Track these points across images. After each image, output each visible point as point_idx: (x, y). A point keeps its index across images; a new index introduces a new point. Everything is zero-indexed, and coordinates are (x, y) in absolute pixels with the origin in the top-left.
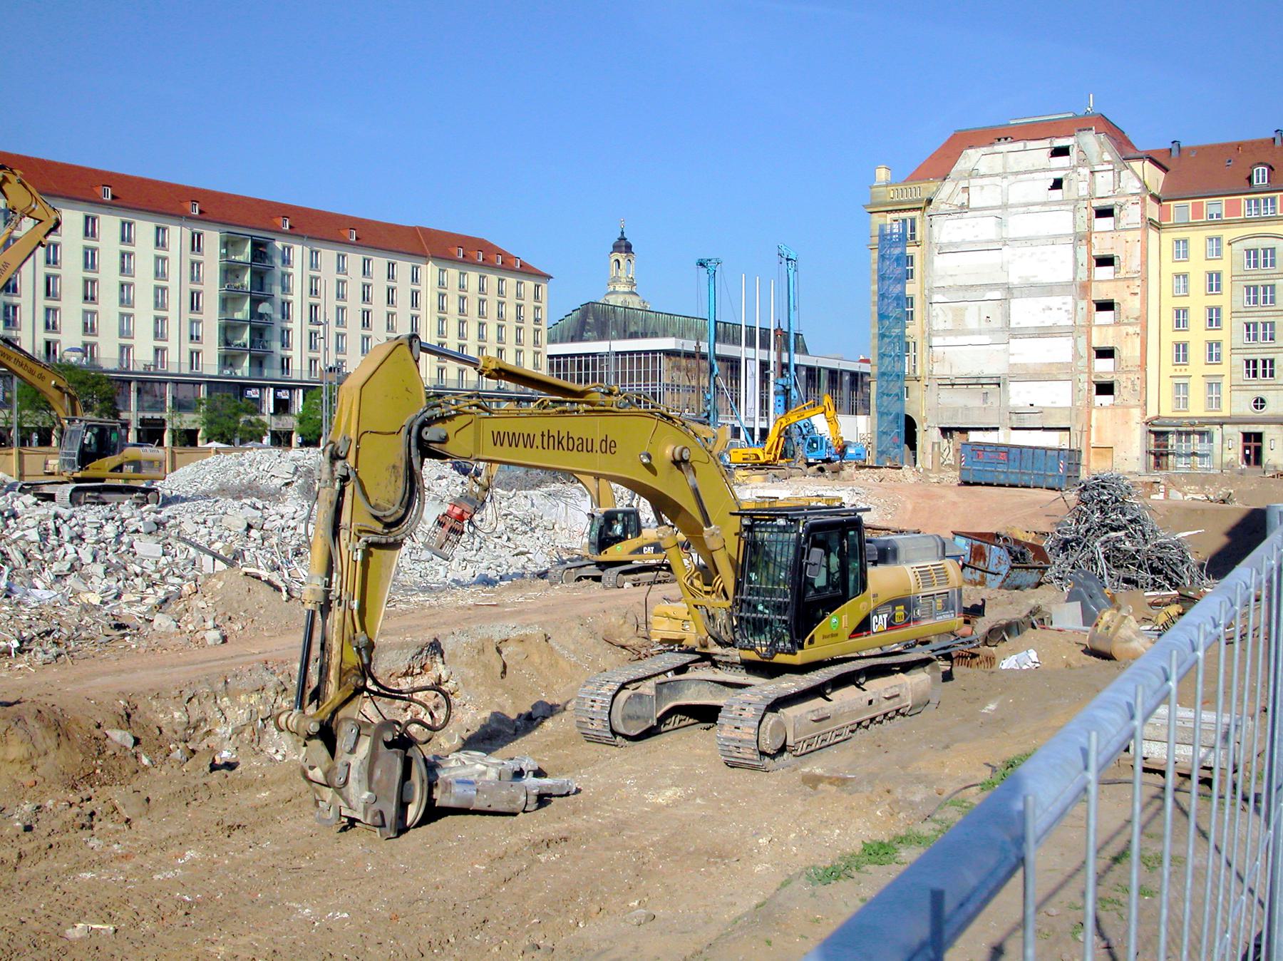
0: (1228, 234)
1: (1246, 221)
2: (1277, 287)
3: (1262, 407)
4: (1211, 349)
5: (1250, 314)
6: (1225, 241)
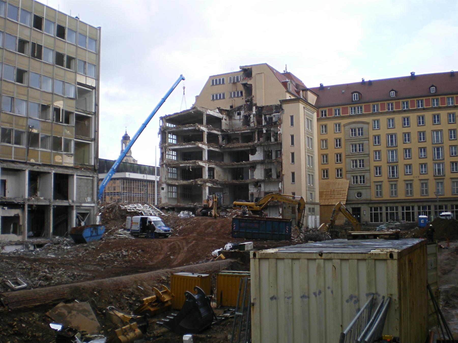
0: (343, 122)
1: (350, 116)
2: (364, 145)
3: (360, 196)
4: (338, 172)
5: (354, 156)
6: (342, 124)
